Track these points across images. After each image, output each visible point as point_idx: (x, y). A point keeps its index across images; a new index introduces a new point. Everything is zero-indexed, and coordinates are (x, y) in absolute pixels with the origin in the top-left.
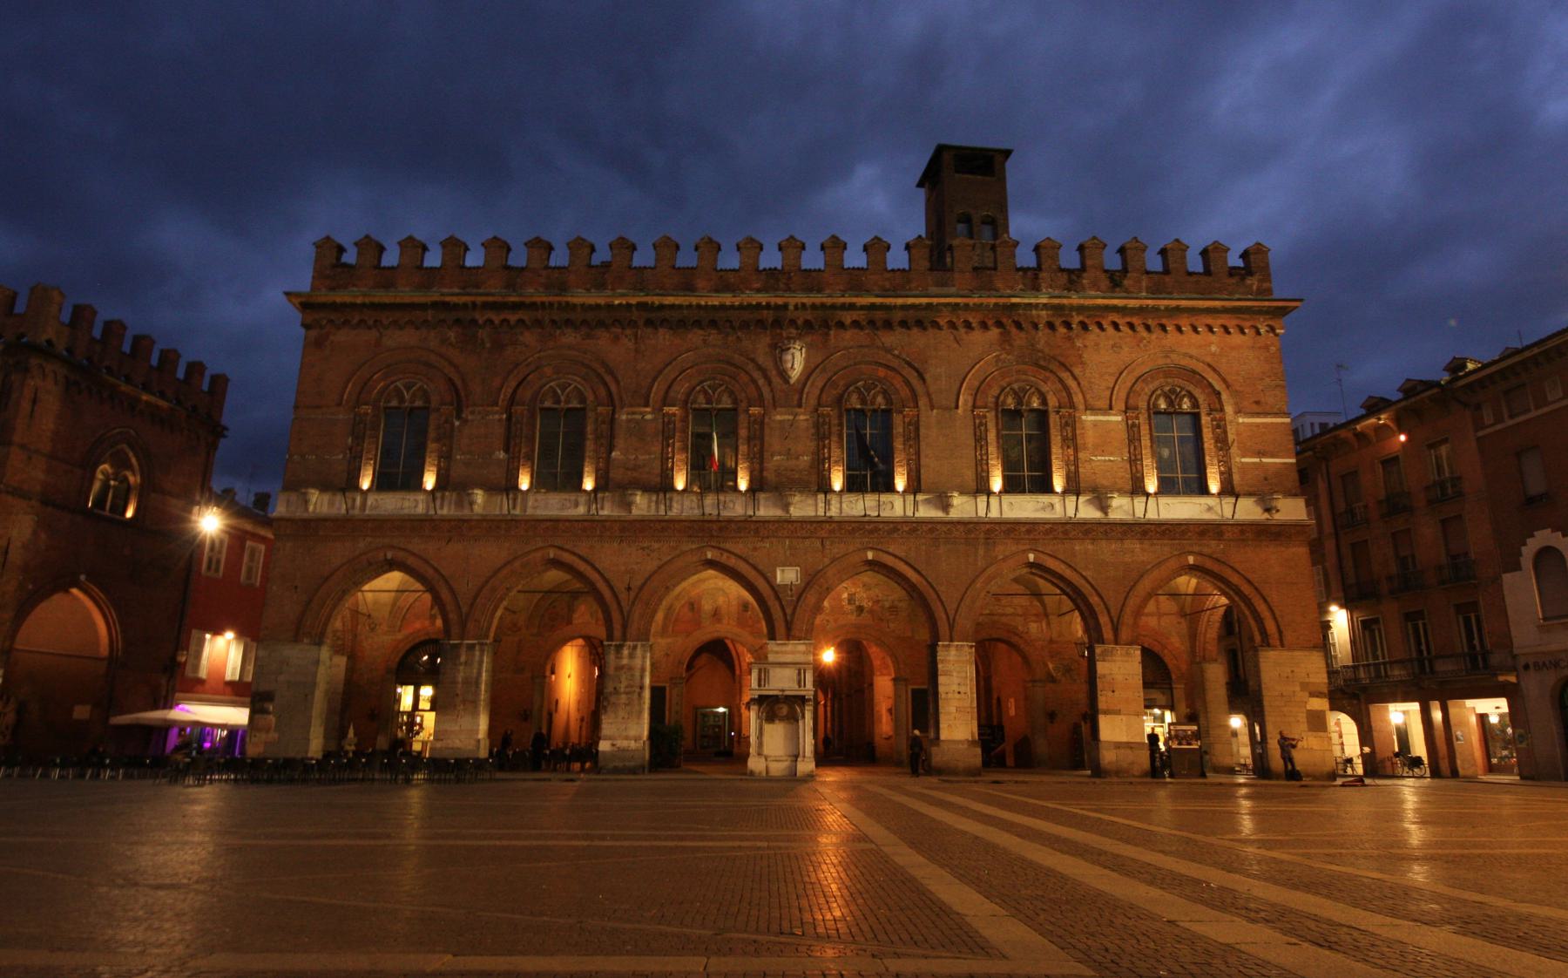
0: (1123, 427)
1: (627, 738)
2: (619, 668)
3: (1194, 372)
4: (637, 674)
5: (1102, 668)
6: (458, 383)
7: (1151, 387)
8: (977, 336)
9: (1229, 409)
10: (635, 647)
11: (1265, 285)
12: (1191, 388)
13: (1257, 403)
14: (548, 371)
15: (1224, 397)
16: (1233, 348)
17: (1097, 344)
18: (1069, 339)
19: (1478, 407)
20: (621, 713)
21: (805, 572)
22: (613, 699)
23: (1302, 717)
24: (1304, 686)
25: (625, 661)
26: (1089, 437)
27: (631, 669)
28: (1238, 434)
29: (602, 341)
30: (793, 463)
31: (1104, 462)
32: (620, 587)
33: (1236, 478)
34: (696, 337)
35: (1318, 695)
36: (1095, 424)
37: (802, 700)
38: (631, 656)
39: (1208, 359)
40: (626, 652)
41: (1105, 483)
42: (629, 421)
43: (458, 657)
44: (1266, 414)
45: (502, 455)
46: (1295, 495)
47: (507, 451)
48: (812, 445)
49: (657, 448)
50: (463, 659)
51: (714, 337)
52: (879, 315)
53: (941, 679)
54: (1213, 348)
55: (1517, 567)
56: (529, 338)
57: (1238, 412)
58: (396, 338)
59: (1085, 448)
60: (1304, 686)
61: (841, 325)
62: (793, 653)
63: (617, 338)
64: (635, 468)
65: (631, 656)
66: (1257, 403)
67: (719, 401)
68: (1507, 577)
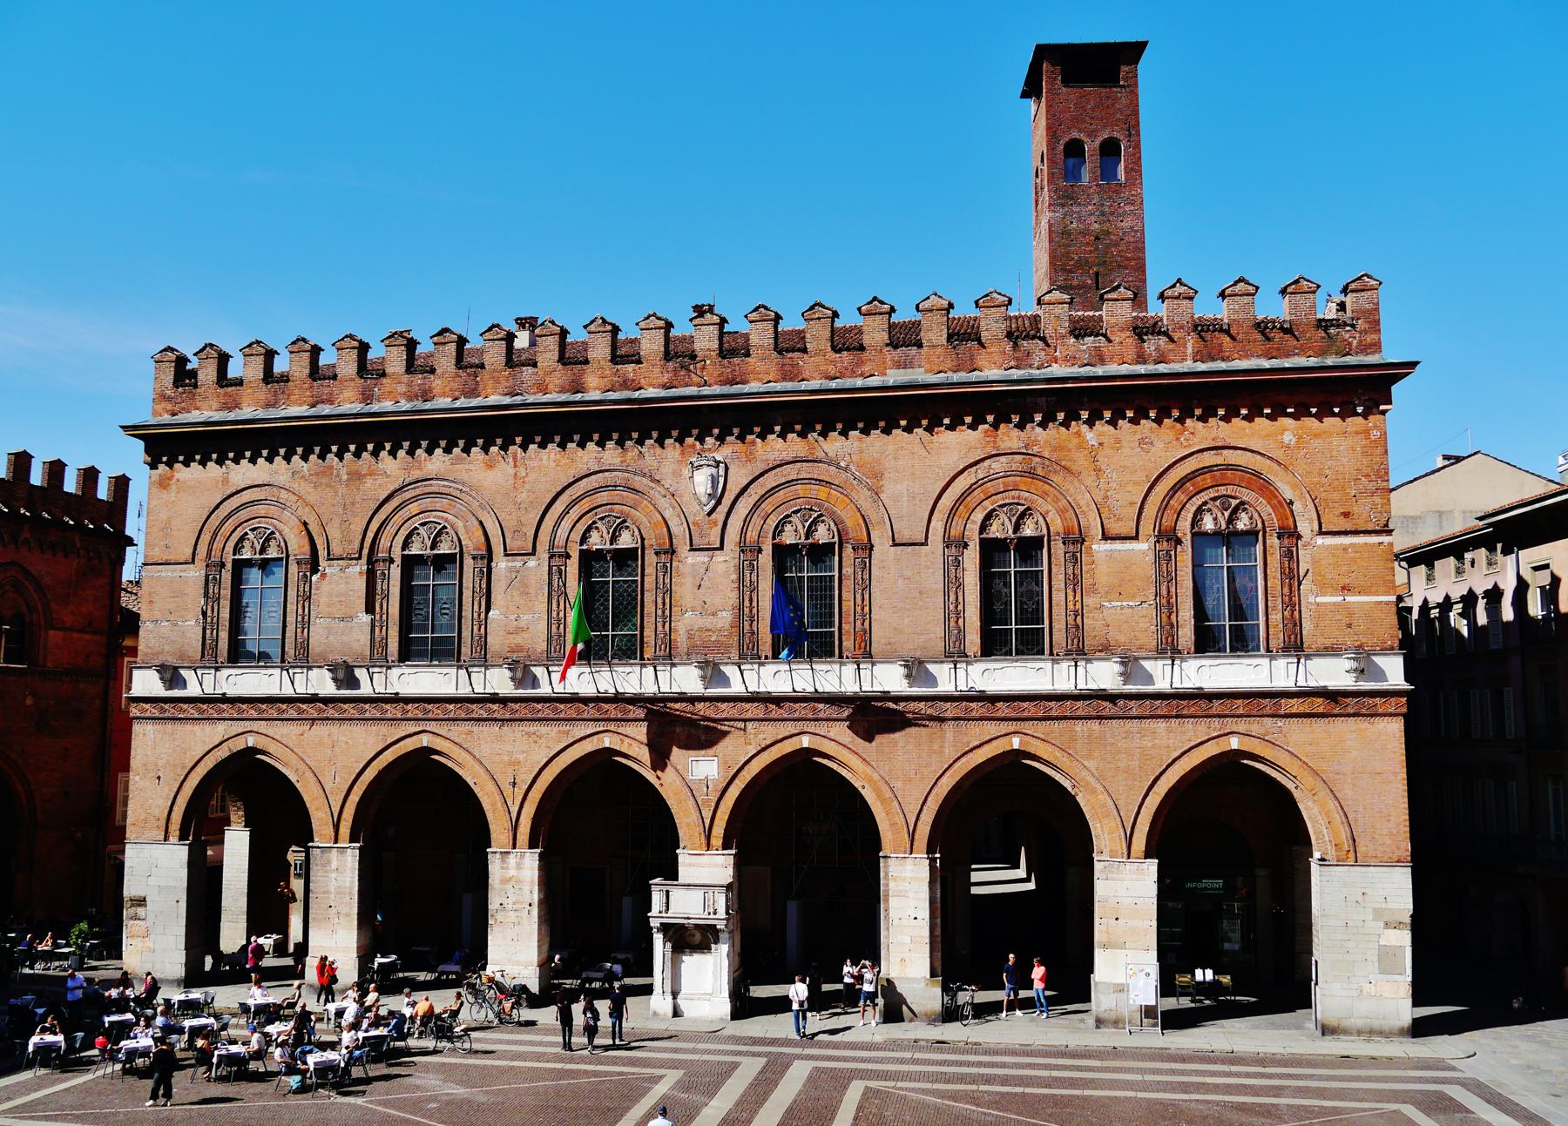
0: (1150, 558)
1: (518, 963)
2: (505, 881)
3: (1257, 474)
4: (526, 888)
6: (314, 528)
7: (1197, 501)
9: (1305, 527)
10: (522, 855)
11: (1370, 338)
12: (1247, 495)
13: (1346, 515)
14: (414, 508)
15: (1297, 507)
16: (1316, 436)
17: (1119, 442)
18: (1078, 434)
22: (499, 917)
23: (1373, 956)
24: (1378, 913)
25: (512, 872)
27: (518, 881)
28: (1315, 561)
30: (707, 622)
33: (1307, 626)
34: (588, 456)
35: (1398, 925)
36: (1110, 555)
38: (519, 866)
39: (1278, 454)
40: (512, 860)
41: (1122, 638)
42: (510, 570)
43: (329, 862)
44: (1356, 533)
45: (367, 618)
46: (1392, 648)
47: (370, 609)
48: (732, 597)
50: (334, 865)
53: (893, 902)
54: (1288, 437)
57: (1321, 533)
58: (244, 472)
60: (1378, 913)
62: (709, 865)
64: (519, 630)
65: (519, 866)
66: (1346, 515)
67: (614, 539)
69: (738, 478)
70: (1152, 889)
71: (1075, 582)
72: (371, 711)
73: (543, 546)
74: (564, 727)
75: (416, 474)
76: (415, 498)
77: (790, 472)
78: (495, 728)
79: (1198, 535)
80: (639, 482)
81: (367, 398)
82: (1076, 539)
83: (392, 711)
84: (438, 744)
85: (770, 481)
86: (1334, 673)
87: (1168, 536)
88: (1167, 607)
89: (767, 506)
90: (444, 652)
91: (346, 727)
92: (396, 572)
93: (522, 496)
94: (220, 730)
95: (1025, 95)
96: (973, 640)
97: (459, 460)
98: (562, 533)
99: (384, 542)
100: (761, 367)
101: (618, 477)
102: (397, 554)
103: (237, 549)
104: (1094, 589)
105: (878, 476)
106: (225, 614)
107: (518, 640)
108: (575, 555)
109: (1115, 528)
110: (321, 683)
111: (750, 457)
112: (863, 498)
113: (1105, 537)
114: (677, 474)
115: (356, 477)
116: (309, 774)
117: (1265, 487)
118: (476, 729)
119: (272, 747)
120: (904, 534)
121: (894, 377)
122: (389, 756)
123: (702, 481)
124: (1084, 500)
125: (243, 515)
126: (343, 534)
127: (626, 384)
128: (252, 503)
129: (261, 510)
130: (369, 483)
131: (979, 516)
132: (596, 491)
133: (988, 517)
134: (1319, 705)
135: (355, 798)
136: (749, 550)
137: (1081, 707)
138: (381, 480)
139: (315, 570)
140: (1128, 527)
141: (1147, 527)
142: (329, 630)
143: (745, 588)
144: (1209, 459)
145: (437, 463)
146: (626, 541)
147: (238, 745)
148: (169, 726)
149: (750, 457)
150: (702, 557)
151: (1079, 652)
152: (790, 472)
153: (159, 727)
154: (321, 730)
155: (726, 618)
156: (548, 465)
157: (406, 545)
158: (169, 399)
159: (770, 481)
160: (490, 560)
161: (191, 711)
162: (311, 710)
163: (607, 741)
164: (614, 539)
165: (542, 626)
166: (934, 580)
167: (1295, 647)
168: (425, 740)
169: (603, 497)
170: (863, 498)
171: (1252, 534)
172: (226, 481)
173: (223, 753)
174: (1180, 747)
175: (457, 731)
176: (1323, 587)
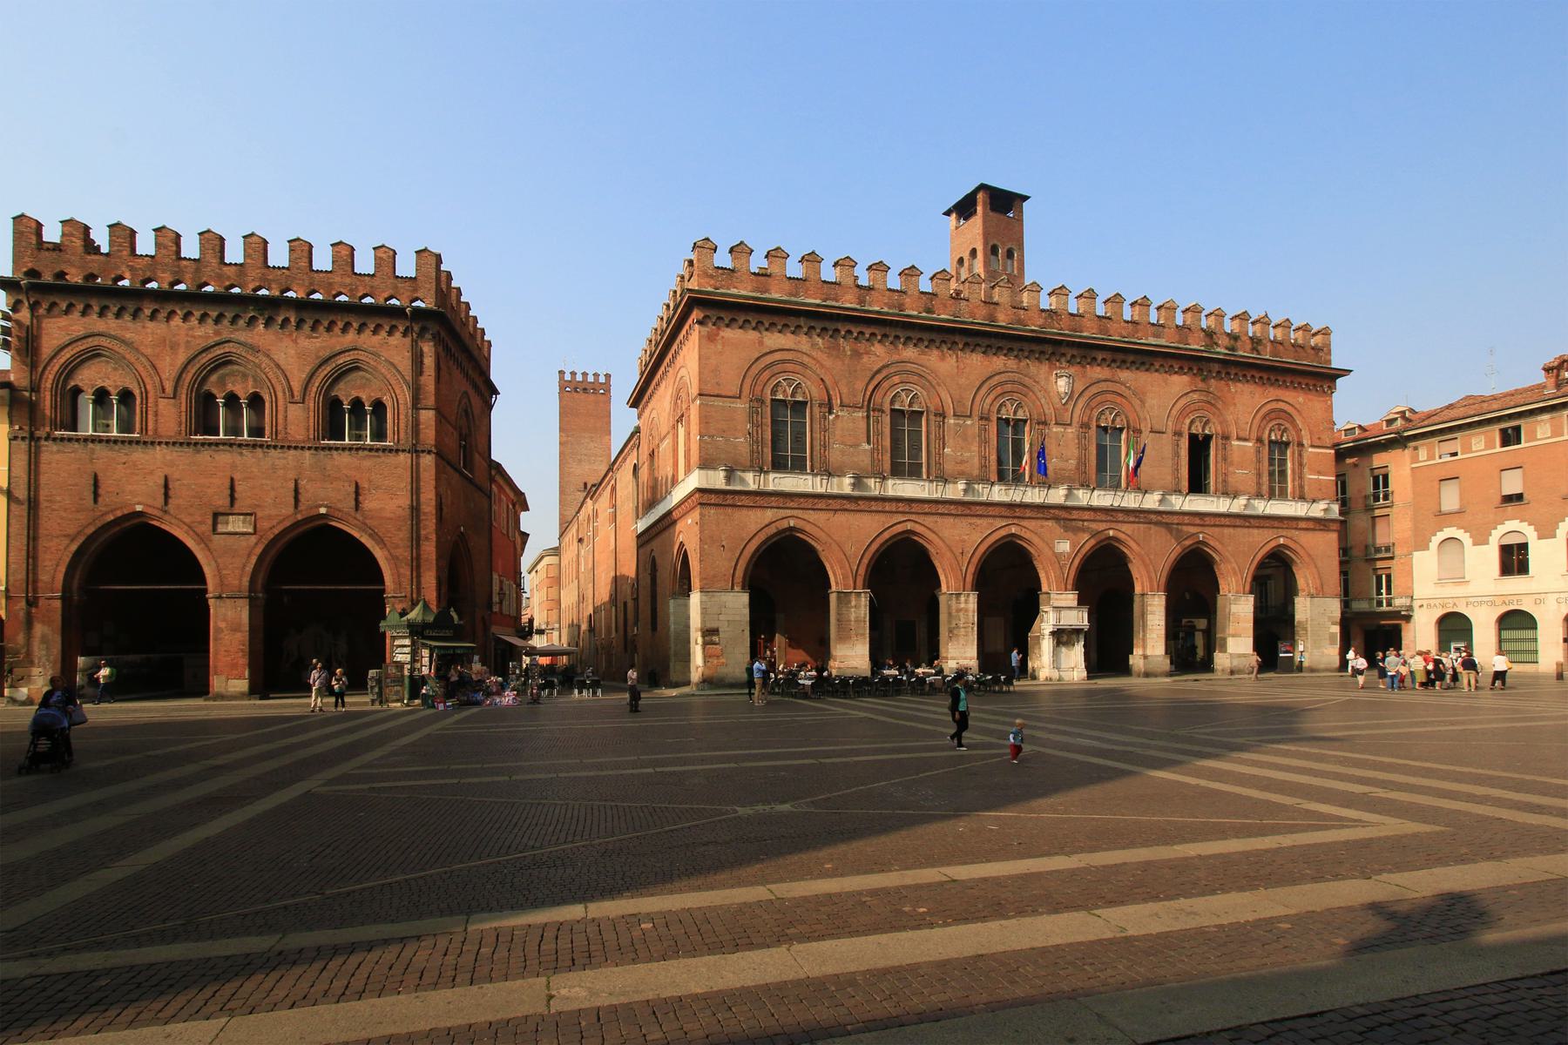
5: (1234, 608)
8: (1175, 378)
14: (896, 379)
19: (1416, 448)
20: (962, 641)
21: (1073, 545)
26: (1235, 457)
27: (966, 610)
29: (934, 355)
30: (1062, 465)
31: (1242, 474)
32: (958, 553)
34: (999, 362)
37: (1078, 631)
38: (966, 602)
40: (963, 598)
45: (867, 447)
49: (975, 448)
51: (1012, 363)
52: (1120, 356)
53: (1149, 617)
55: (1427, 548)
56: (878, 349)
58: (774, 340)
59: (1232, 464)
61: (1094, 359)
63: (943, 358)
64: (962, 462)
67: (1015, 413)
68: (1416, 554)
69: (1079, 387)
70: (1251, 609)
71: (1225, 459)
72: (874, 506)
73: (976, 413)
74: (990, 520)
75: (896, 358)
76: (896, 374)
77: (1103, 386)
78: (951, 520)
79: (1271, 442)
80: (1027, 381)
81: (862, 302)
82: (1226, 438)
83: (888, 507)
84: (919, 529)
85: (1094, 390)
86: (1317, 510)
87: (1259, 440)
88: (1259, 475)
89: (1093, 404)
90: (914, 472)
91: (858, 515)
92: (887, 419)
93: (962, 381)
94: (769, 515)
95: (948, 213)
96: (1185, 484)
97: (923, 353)
98: (986, 407)
99: (877, 397)
100: (1088, 324)
101: (1016, 377)
102: (887, 407)
103: (774, 392)
104: (1232, 464)
105: (1144, 394)
106: (768, 435)
107: (962, 468)
108: (994, 419)
109: (1242, 434)
110: (845, 485)
111: (1084, 376)
112: (1136, 402)
113: (1239, 439)
114: (1047, 379)
115: (857, 354)
116: (834, 546)
117: (1295, 425)
118: (938, 519)
119: (808, 528)
120: (1156, 428)
121: (1152, 341)
122: (887, 535)
123: (1062, 385)
124: (1230, 418)
125: (780, 367)
126: (852, 387)
127: (1020, 322)
128: (783, 361)
129: (789, 366)
130: (865, 359)
131: (1188, 421)
132: (1006, 382)
133: (1192, 422)
134: (1311, 525)
135: (865, 561)
136: (1085, 426)
137: (1227, 521)
138: (873, 358)
139: (830, 412)
140: (1245, 434)
141: (1254, 435)
142: (843, 452)
143: (1083, 448)
144: (1274, 405)
145: (910, 352)
146: (1020, 415)
147: (784, 524)
148: (729, 510)
149: (1084, 376)
150: (1060, 429)
151: (1229, 493)
152: (1103, 386)
153: (721, 510)
154: (841, 518)
155: (1073, 462)
156: (977, 364)
157: (892, 402)
158: (711, 277)
159: (1094, 390)
160: (943, 415)
161: (746, 500)
162: (834, 504)
163: (1013, 530)
164: (1015, 413)
165: (976, 460)
166: (1168, 451)
167: (1302, 498)
168: (909, 526)
169: (1008, 387)
170: (1136, 402)
171: (1287, 444)
172: (761, 343)
173: (772, 530)
174: (1262, 541)
175: (929, 521)
176: (1312, 472)
